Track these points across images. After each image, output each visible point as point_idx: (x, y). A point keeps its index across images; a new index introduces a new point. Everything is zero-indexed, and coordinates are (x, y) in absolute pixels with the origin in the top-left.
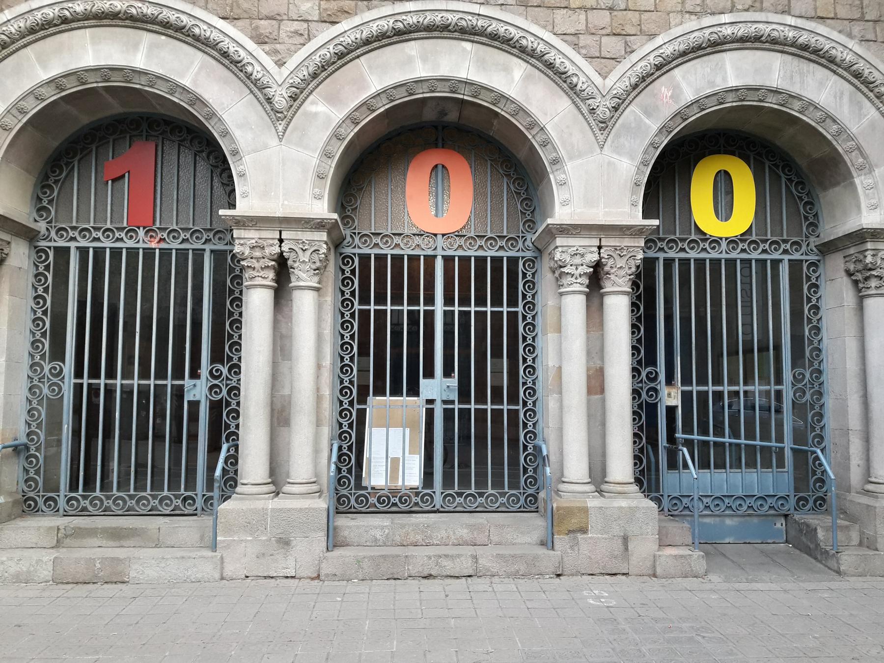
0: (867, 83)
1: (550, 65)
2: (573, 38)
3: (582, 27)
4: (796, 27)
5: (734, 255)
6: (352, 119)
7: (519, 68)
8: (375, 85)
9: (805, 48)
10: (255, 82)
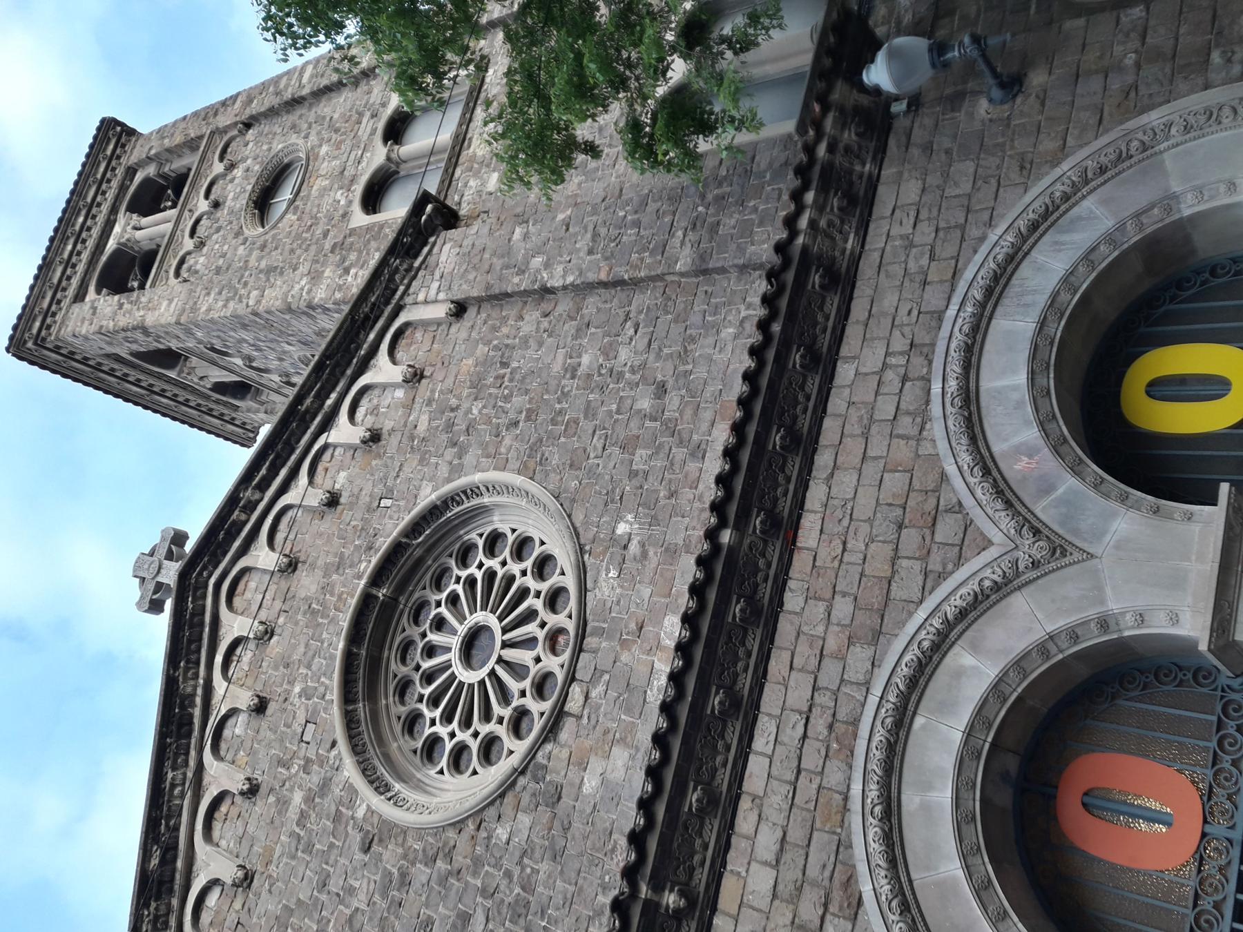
0: (1046, 214)
1: (962, 614)
2: (931, 579)
3: (917, 566)
4: (962, 304)
7: (960, 657)
8: (953, 868)
9: (989, 292)
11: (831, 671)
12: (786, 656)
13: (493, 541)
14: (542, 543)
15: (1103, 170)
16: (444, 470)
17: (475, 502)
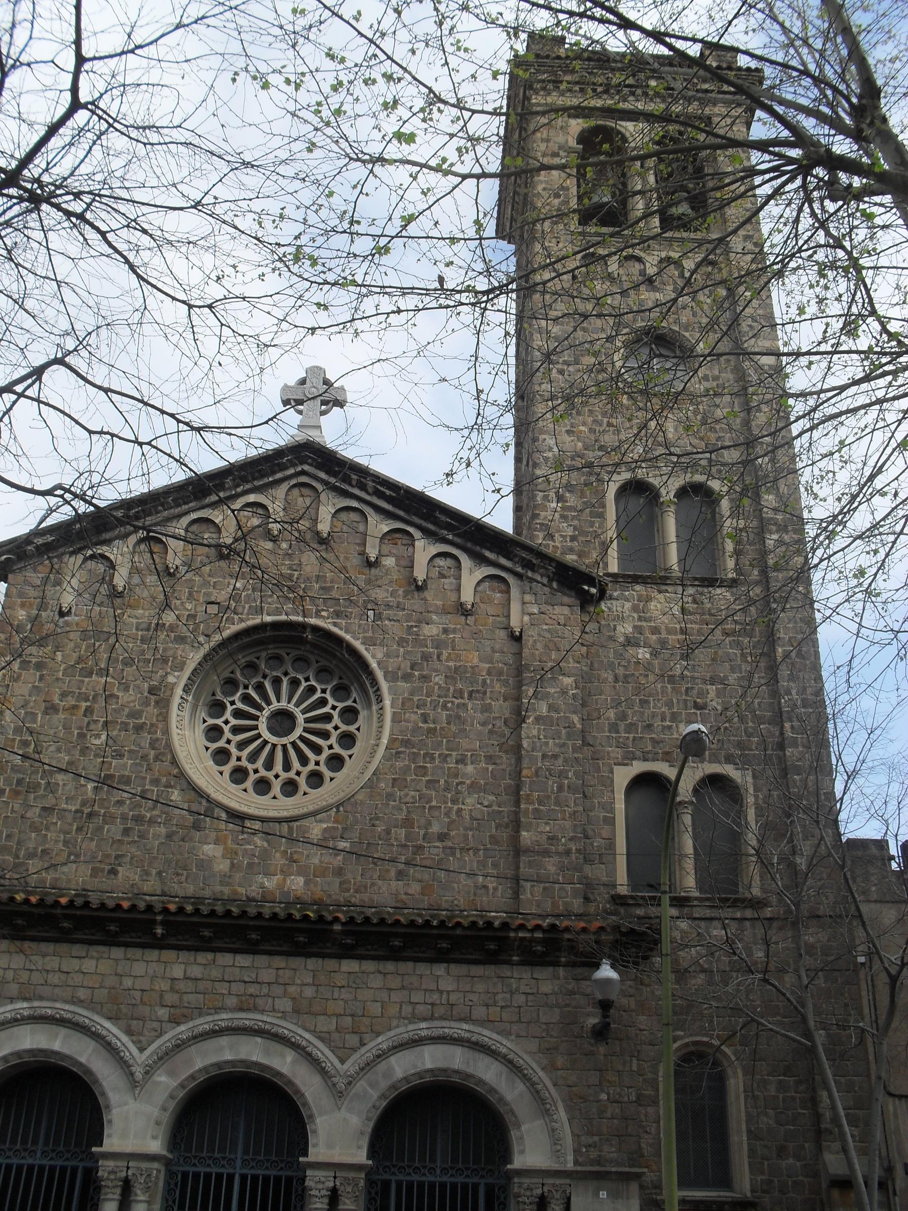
1: (310, 1055)
3: (333, 1027)
5: (445, 1179)
6: (182, 1086)
7: (290, 1056)
8: (199, 1064)
9: (476, 1043)
10: (125, 1062)
11: (278, 990)
12: (283, 965)
13: (350, 714)
14: (350, 756)
15: (538, 1092)
16: (392, 664)
17: (373, 699)
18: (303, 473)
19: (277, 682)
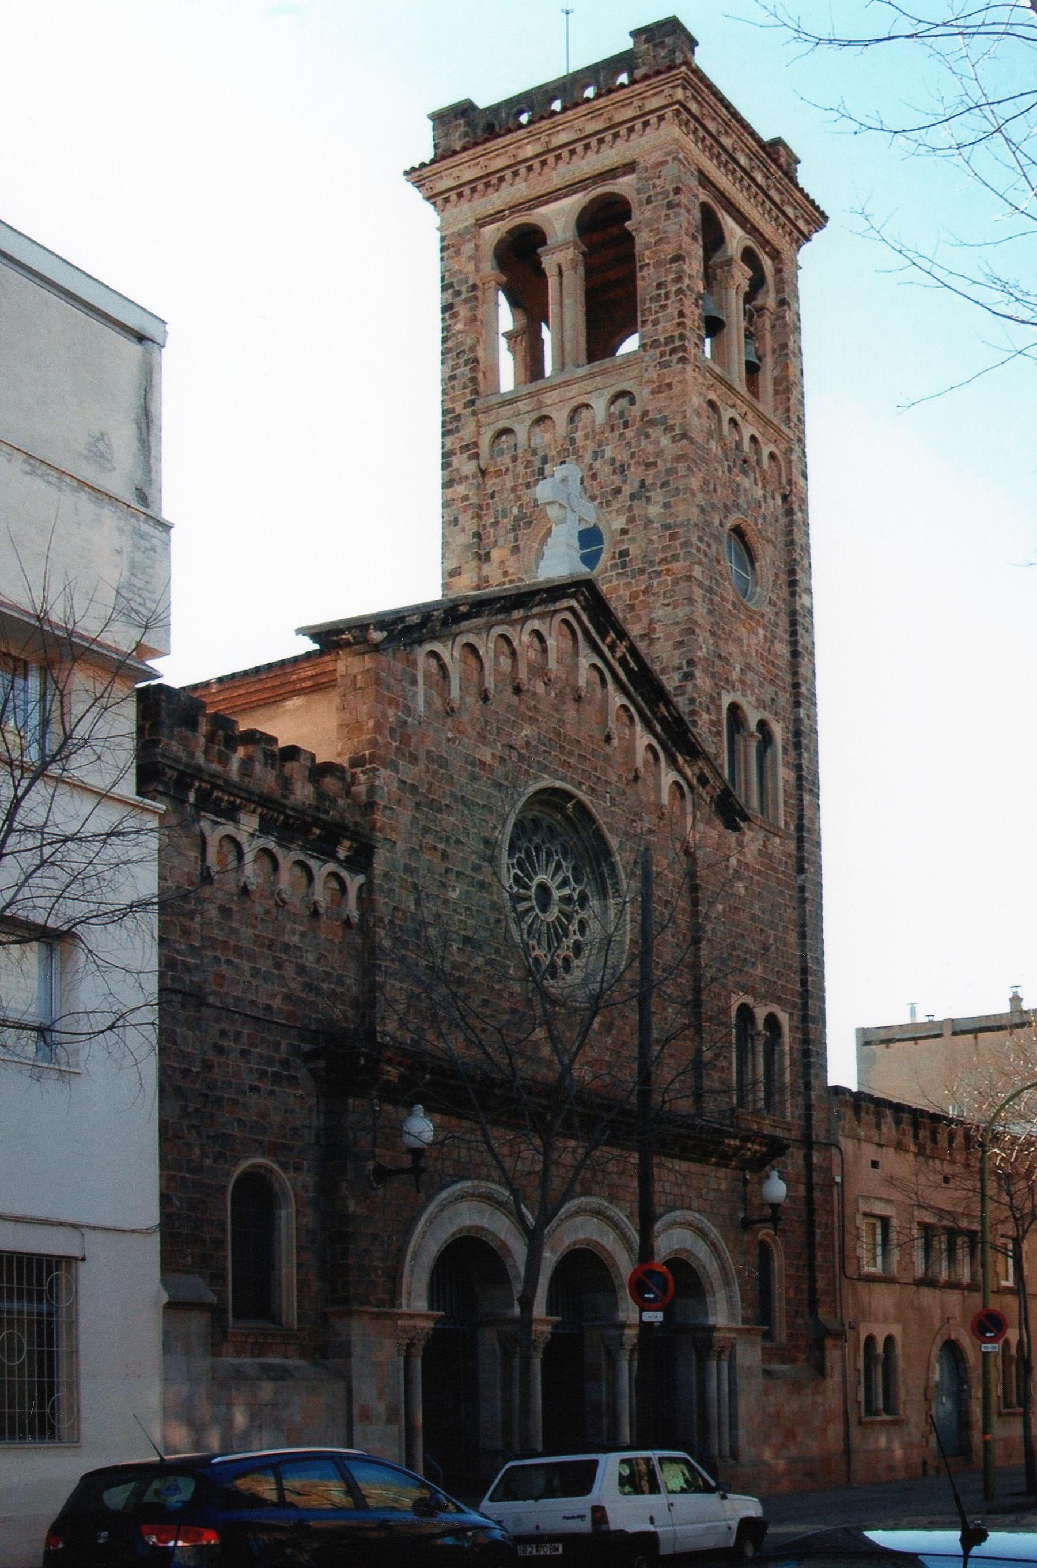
18: (571, 609)
19: (538, 849)
